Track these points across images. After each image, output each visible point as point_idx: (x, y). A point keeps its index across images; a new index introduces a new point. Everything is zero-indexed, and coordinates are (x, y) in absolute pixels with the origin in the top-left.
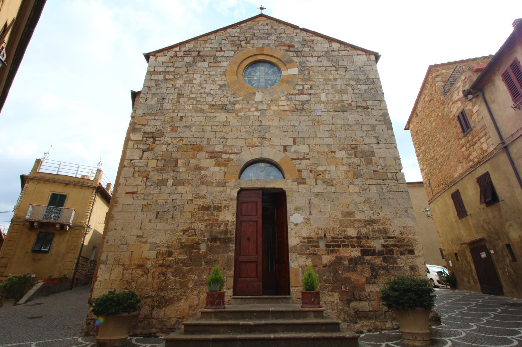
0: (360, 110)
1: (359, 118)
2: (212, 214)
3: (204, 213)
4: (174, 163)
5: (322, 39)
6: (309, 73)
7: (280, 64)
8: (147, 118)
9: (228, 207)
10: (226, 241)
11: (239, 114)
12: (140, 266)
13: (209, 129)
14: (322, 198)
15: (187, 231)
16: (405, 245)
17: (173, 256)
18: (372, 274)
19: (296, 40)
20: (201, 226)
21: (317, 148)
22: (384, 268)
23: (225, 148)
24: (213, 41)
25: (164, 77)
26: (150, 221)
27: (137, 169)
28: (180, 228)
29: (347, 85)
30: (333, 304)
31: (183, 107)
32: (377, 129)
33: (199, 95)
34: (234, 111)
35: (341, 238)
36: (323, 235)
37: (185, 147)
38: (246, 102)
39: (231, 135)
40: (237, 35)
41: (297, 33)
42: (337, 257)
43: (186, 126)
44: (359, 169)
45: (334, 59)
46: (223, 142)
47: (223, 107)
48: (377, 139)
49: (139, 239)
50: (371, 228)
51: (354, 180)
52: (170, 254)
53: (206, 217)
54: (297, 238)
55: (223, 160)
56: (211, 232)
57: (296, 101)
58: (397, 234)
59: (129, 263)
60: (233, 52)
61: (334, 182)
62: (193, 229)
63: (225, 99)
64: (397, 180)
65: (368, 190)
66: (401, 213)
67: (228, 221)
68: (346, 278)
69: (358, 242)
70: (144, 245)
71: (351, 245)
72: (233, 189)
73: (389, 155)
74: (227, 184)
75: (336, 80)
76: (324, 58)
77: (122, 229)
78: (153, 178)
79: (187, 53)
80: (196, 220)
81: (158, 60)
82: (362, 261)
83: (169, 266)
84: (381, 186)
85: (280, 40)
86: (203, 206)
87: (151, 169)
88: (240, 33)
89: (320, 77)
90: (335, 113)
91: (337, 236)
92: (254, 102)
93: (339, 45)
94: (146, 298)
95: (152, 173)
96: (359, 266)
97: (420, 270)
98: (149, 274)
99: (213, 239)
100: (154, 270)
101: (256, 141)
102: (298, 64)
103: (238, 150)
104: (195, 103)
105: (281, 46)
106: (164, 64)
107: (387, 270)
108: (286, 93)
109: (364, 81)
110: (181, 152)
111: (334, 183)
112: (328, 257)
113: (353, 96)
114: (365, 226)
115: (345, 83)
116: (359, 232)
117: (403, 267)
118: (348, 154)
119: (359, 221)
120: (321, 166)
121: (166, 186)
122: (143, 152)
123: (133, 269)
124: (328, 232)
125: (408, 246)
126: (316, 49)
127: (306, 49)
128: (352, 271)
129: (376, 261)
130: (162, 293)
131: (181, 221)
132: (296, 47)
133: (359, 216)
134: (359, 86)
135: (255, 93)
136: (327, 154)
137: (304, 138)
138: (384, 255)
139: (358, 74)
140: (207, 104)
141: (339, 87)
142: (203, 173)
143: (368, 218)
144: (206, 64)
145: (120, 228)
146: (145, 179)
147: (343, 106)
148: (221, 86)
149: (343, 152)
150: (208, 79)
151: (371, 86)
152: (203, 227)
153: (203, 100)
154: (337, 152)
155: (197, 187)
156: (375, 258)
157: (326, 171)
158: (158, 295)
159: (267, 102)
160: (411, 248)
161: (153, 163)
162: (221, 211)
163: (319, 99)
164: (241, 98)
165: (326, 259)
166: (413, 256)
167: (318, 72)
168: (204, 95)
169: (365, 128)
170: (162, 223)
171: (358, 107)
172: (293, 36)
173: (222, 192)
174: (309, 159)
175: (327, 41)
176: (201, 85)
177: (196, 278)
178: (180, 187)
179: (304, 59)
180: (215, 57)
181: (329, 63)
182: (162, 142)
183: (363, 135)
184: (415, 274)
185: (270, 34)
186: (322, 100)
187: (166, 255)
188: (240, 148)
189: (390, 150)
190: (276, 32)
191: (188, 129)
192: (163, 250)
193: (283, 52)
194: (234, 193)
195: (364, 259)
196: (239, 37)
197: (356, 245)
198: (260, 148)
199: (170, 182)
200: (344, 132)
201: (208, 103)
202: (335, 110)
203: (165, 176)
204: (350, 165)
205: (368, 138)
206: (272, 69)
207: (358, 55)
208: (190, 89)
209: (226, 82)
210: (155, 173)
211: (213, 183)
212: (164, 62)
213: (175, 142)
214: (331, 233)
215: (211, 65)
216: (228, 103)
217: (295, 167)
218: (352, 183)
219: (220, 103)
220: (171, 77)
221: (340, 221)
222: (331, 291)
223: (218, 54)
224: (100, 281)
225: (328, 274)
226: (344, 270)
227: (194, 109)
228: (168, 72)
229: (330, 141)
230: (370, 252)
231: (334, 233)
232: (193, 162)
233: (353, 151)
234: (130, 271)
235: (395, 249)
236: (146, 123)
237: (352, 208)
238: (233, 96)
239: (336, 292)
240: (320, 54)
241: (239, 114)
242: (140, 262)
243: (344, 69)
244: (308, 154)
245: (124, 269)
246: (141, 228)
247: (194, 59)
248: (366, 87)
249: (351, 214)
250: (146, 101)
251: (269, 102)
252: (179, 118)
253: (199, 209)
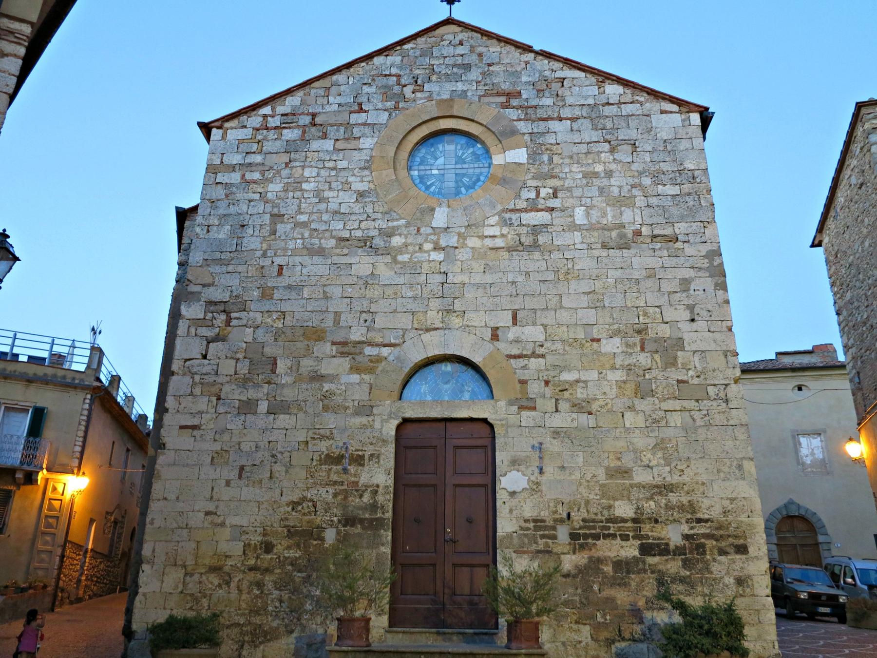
0: (659, 245)
1: (654, 262)
2: (345, 471)
3: (330, 470)
4: (270, 366)
5: (583, 74)
6: (551, 160)
7: (489, 140)
8: (211, 269)
9: (378, 457)
10: (375, 525)
11: (400, 258)
12: (215, 569)
13: (336, 292)
14: (567, 440)
15: (298, 503)
16: (729, 536)
17: (275, 551)
18: (659, 591)
19: (524, 79)
20: (326, 494)
21: (562, 332)
22: (682, 580)
23: (370, 335)
24: (342, 88)
25: (243, 176)
26: (228, 483)
27: (197, 378)
28: (285, 499)
29: (632, 186)
30: (578, 646)
31: (283, 244)
32: (692, 288)
33: (314, 217)
34: (387, 251)
35: (602, 522)
36: (565, 516)
37: (288, 332)
38: (413, 230)
39: (381, 306)
40: (394, 71)
41: (527, 63)
42: (590, 558)
43: (289, 287)
44: (647, 376)
45: (609, 125)
46: (366, 321)
47: (365, 243)
48: (692, 312)
49: (209, 518)
50: (664, 501)
51: (637, 402)
52: (268, 548)
53: (334, 477)
54: (514, 521)
55: (367, 359)
56: (345, 507)
57: (521, 225)
58: (715, 513)
59: (194, 563)
60: (387, 114)
61: (593, 406)
62: (311, 500)
63: (370, 224)
64: (727, 401)
65: (663, 423)
66: (727, 469)
67: (378, 486)
68: (607, 598)
69: (635, 530)
70: (217, 530)
71: (620, 535)
72: (387, 421)
73: (713, 346)
74: (375, 411)
75: (609, 174)
76: (587, 123)
77: (178, 498)
78: (230, 397)
79: (289, 119)
80: (315, 484)
81: (229, 137)
82: (641, 566)
83: (267, 570)
84: (692, 413)
85: (488, 81)
86: (327, 455)
87: (225, 379)
88: (400, 67)
89: (575, 168)
90: (604, 253)
91: (593, 517)
92: (429, 231)
93: (620, 89)
94: (228, 627)
95: (226, 388)
96: (633, 576)
97: (756, 585)
98: (232, 585)
99: (349, 521)
100: (241, 576)
101: (434, 317)
102: (527, 137)
103: (396, 337)
104: (306, 235)
105: (491, 95)
106: (241, 146)
107: (688, 583)
108: (499, 207)
109: (672, 175)
110: (281, 344)
111: (595, 407)
112: (574, 557)
113: (646, 212)
114: (652, 498)
115: (631, 181)
116: (638, 508)
117: (722, 578)
118: (628, 345)
119: (640, 486)
120: (569, 371)
121: (255, 413)
122: (208, 343)
123: (202, 574)
124: (576, 509)
125: (736, 537)
126: (570, 100)
127: (548, 101)
128: (619, 585)
129: (669, 566)
130: (257, 620)
131: (285, 484)
132: (524, 96)
133: (641, 477)
134: (660, 187)
135: (433, 210)
136: (582, 346)
137: (534, 310)
138: (685, 554)
139: (661, 158)
140: (332, 237)
141: (615, 191)
142: (327, 387)
143: (658, 481)
144: (328, 145)
145: (174, 497)
146: (214, 399)
147: (622, 236)
148: (361, 195)
149: (617, 341)
150: (334, 179)
151: (687, 188)
152: (330, 498)
153: (324, 228)
154: (603, 341)
155: (316, 415)
156: (667, 560)
157: (577, 381)
158: (250, 623)
159: (457, 230)
160: (741, 542)
161: (227, 367)
162: (363, 465)
163: (570, 219)
164: (402, 222)
165: (570, 562)
166: (744, 557)
167: (571, 157)
168: (325, 217)
169: (666, 287)
170: (252, 489)
171: (655, 236)
172: (519, 69)
173: (364, 427)
174: (543, 356)
175: (593, 79)
176: (318, 193)
177: (318, 593)
178: (282, 416)
179: (542, 126)
180: (348, 126)
181: (595, 136)
182: (244, 322)
183: (663, 301)
184: (744, 591)
185: (467, 67)
186: (577, 222)
187: (261, 548)
188: (401, 333)
189: (717, 336)
190: (481, 61)
191: (294, 293)
192: (256, 539)
193: (494, 111)
194: (390, 429)
195: (644, 562)
196: (399, 76)
197: (631, 534)
198: (441, 332)
199: (263, 407)
200: (620, 296)
201: (334, 233)
202: (605, 246)
203: (252, 394)
204: (629, 369)
205: (672, 309)
206: (471, 150)
207: (662, 112)
208: (296, 202)
209: (372, 186)
210: (234, 387)
211: (347, 408)
212: (241, 142)
213: (269, 320)
214: (583, 510)
215: (340, 145)
216: (375, 233)
217: (515, 373)
218: (631, 408)
219: (359, 234)
220: (256, 176)
221: (603, 486)
222: (577, 622)
223: (355, 118)
224: (144, 595)
225: (571, 590)
226: (604, 583)
227: (305, 247)
228: (250, 165)
229: (590, 316)
230: (662, 549)
231: (588, 511)
232: (307, 364)
233: (637, 339)
234: (196, 577)
235: (710, 543)
236: (210, 281)
237: (627, 461)
238: (387, 217)
239: (585, 624)
240: (577, 112)
241: (400, 258)
242: (214, 562)
243: (629, 148)
244: (542, 346)
245: (186, 574)
246: (212, 498)
247: (304, 132)
248: (675, 190)
249: (625, 472)
250: (208, 231)
251: (463, 230)
252: (276, 269)
253: (321, 462)
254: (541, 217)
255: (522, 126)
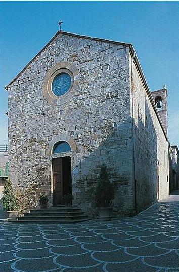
108: (72, 96)
165: (87, 189)
223: (38, 76)
254: (82, 97)
255: (78, 67)
